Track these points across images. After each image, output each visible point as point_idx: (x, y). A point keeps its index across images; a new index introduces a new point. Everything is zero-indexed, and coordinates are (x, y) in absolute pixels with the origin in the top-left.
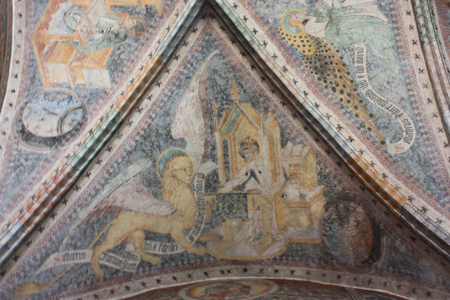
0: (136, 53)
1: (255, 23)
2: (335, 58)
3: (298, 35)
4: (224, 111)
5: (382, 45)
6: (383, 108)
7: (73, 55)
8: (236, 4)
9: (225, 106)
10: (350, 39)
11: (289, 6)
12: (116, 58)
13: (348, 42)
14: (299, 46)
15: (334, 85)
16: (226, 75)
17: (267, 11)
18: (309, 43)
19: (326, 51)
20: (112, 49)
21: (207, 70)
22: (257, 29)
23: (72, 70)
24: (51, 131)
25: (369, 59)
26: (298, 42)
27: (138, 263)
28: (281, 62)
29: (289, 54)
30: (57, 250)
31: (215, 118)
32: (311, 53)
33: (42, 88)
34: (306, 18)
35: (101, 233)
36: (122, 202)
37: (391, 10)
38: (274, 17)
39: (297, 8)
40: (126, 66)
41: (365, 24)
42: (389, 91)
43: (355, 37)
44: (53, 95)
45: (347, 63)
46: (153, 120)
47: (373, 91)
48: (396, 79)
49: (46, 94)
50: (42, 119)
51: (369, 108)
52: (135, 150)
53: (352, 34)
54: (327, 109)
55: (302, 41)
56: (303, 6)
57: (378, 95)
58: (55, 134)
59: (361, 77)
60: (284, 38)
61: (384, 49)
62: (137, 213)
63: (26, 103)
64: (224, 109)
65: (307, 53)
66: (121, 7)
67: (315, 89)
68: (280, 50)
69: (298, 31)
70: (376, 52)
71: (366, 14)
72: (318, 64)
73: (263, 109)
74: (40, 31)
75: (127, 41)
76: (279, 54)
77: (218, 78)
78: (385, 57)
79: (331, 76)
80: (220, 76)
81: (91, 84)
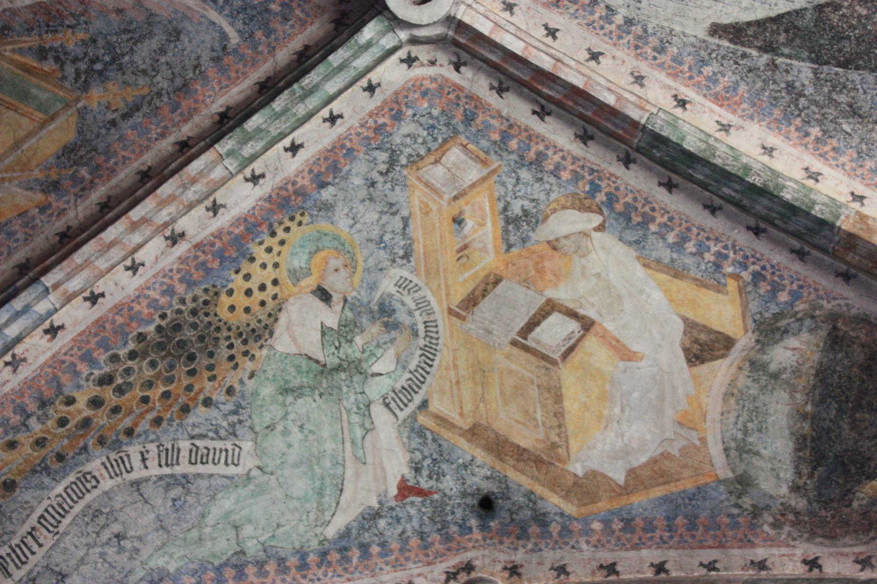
1: (320, 147)
2: (208, 385)
3: (282, 274)
4: (56, 67)
5: (250, 521)
6: (33, 520)
8: (378, 90)
9: (70, 70)
10: (271, 427)
11: (372, 246)
13: (260, 421)
14: (247, 277)
15: (120, 381)
16: (164, 67)
17: (357, 181)
18: (256, 308)
19: (231, 358)
21: (176, 12)
22: (302, 154)
25: (203, 483)
26: (260, 276)
28: (196, 225)
29: (222, 251)
31: (33, 40)
32: (224, 314)
34: (336, 297)
37: (364, 548)
38: (340, 204)
39: (367, 270)
41: (318, 471)
42: (89, 540)
43: (276, 442)
45: (191, 419)
47: (96, 493)
48: (131, 558)
51: (35, 480)
53: (286, 432)
54: (42, 360)
55: (262, 288)
56: (373, 287)
57: (78, 508)
59: (144, 460)
60: (273, 234)
61: (236, 528)
64: (62, 65)
65: (225, 300)
67: (108, 326)
68: (237, 222)
69: (296, 276)
70: (227, 503)
71: (349, 473)
72: (189, 334)
73: (54, 176)
76: (224, 219)
77: (154, 43)
78: (207, 530)
79: (148, 373)
80: (162, 51)
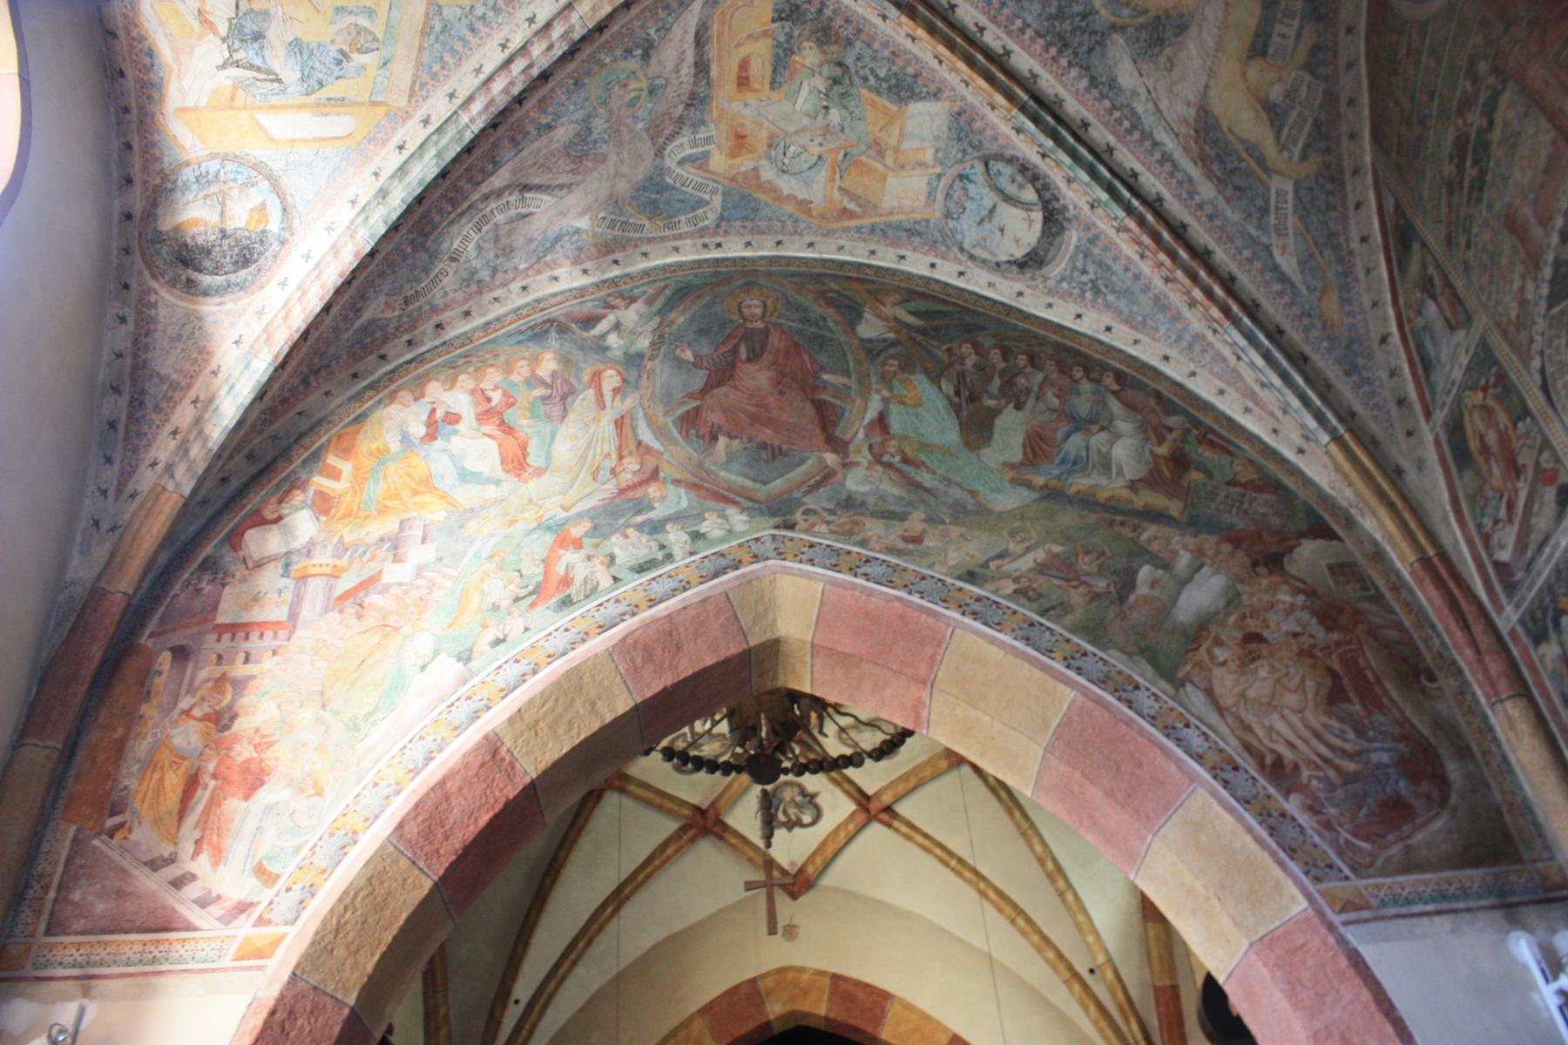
0: (876, 46)
7: (871, 162)
12: (884, 85)
20: (864, 92)
23: (903, 167)
24: (1031, 222)
27: (1308, 78)
30: (1268, 248)
33: (932, 221)
35: (1244, 155)
36: (1189, 105)
40: (904, 68)
44: (951, 205)
46: (1029, 26)
49: (948, 215)
50: (1002, 230)
52: (1088, 69)
58: (1038, 216)
62: (1212, 74)
63: (962, 249)
66: (775, 71)
74: (814, 213)
75: (849, 61)
81: (937, 138)
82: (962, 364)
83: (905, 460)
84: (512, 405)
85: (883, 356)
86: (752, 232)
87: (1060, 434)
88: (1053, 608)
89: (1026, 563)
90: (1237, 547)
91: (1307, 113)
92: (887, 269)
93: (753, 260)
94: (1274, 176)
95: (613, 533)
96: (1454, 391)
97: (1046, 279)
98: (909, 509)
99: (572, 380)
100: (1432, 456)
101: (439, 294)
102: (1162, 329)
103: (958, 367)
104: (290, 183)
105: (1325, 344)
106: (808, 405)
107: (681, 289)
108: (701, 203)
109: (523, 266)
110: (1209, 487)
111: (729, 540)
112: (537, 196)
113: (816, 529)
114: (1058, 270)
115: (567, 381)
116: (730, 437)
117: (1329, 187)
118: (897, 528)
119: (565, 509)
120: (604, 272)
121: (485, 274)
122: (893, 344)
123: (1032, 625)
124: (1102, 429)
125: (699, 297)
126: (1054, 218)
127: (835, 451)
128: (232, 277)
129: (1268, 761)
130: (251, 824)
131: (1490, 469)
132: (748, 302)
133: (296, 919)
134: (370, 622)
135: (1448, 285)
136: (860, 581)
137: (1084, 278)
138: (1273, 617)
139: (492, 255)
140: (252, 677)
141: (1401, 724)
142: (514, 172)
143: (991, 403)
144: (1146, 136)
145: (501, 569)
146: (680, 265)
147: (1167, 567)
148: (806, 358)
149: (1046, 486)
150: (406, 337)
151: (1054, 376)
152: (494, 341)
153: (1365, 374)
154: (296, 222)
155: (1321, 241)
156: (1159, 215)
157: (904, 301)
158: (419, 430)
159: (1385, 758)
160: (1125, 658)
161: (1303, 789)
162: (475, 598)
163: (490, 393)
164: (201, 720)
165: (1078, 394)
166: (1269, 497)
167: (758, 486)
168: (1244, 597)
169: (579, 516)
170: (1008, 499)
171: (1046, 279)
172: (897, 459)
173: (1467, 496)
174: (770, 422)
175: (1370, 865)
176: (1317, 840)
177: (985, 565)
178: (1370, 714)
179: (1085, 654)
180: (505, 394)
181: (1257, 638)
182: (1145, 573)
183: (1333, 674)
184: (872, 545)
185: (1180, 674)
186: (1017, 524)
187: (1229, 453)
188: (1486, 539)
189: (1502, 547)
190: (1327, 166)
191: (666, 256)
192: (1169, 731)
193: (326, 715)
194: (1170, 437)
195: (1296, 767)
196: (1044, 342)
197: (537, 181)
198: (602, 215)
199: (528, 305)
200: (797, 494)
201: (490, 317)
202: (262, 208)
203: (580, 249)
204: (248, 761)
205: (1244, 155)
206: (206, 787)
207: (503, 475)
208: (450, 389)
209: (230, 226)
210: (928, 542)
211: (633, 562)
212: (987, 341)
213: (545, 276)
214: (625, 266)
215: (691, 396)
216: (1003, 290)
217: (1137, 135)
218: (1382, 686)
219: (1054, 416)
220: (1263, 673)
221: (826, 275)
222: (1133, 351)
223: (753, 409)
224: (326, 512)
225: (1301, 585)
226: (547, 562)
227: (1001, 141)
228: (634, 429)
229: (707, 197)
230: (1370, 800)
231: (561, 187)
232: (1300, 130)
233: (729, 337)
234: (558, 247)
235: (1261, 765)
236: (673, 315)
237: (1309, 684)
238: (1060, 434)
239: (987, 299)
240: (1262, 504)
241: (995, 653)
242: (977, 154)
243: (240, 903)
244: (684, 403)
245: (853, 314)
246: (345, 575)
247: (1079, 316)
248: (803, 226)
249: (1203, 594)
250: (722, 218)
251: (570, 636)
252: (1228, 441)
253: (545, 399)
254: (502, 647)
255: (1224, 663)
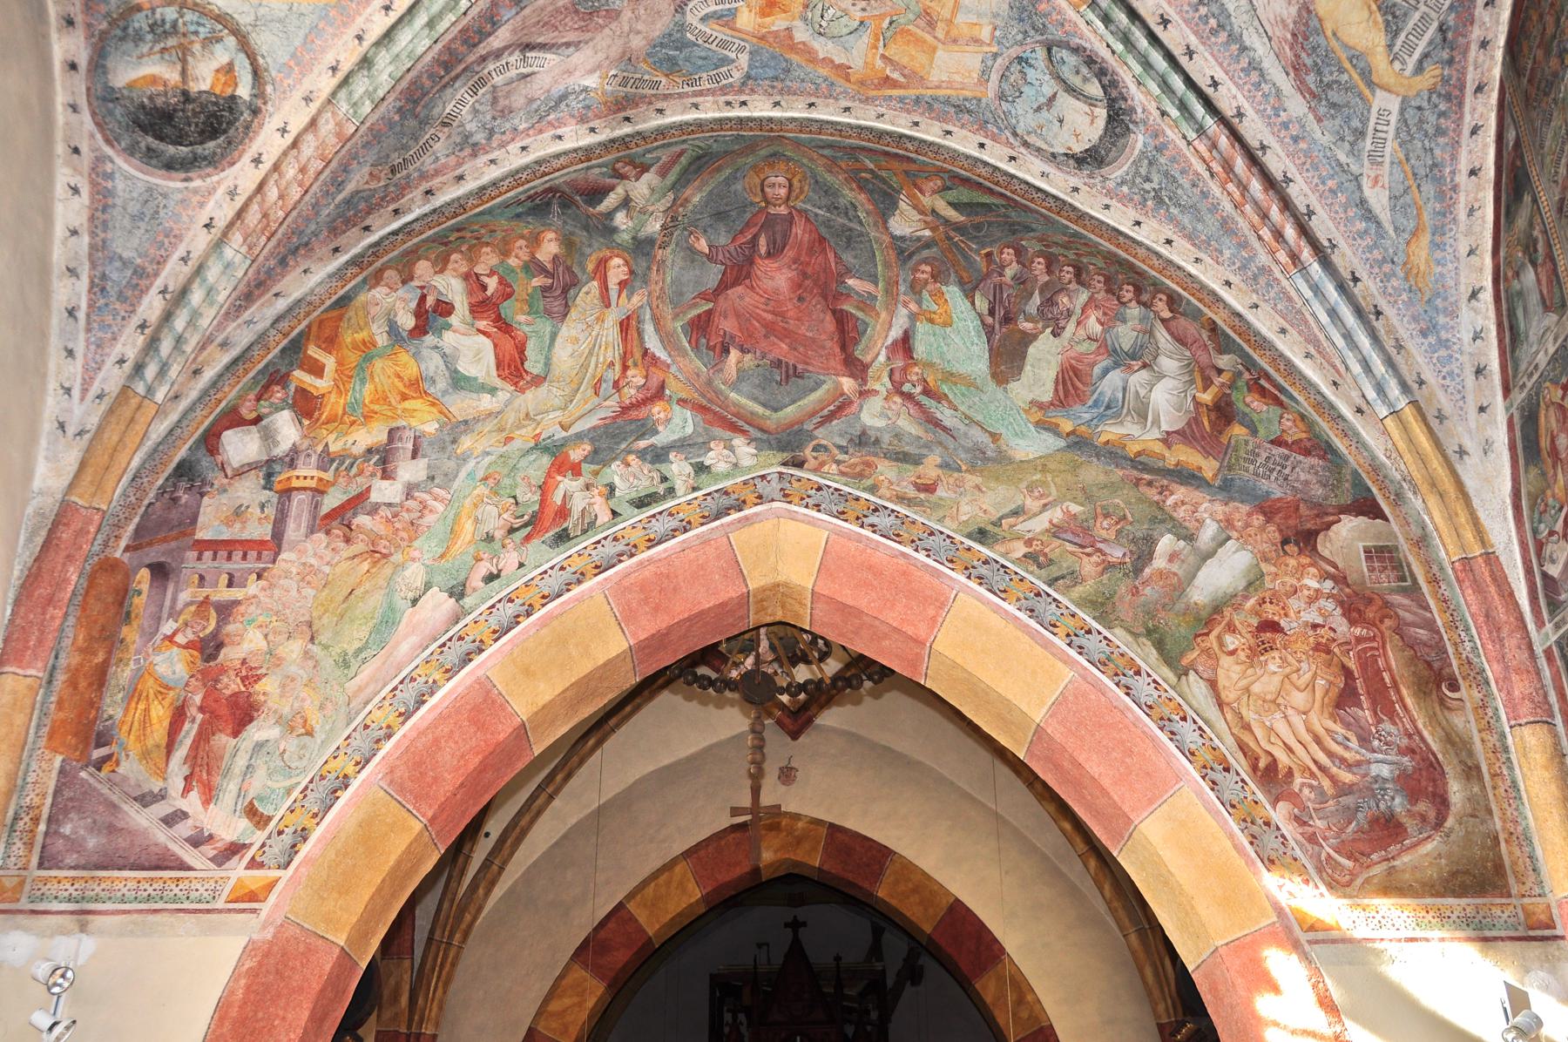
23: (955, 41)
30: (1357, 178)
35: (1347, 65)
44: (1005, 86)
49: (1002, 97)
50: (1061, 121)
58: (1102, 113)
63: (1015, 134)
82: (1001, 275)
83: (927, 392)
84: (509, 296)
85: (916, 258)
86: (781, 92)
87: (1097, 370)
88: (1063, 577)
89: (1039, 524)
90: (1269, 520)
91: (1433, 15)
92: (932, 144)
93: (780, 121)
94: (1378, 92)
95: (615, 459)
96: (1535, 377)
97: (1105, 179)
98: (925, 451)
99: (576, 269)
100: (1501, 436)
101: (429, 161)
102: (1227, 253)
103: (996, 279)
104: (263, 41)
105: (1405, 296)
106: (829, 317)
107: (699, 158)
108: (725, 61)
109: (521, 128)
110: (1250, 447)
111: (734, 476)
112: (541, 55)
113: (826, 468)
114: (1119, 173)
115: (569, 269)
116: (743, 351)
117: (1443, 107)
118: (911, 472)
119: (564, 428)
120: (613, 129)
121: (480, 137)
122: (928, 245)
123: (1038, 595)
124: (1145, 366)
125: (719, 170)
126: (1119, 118)
127: (852, 375)
128: (199, 149)
129: (1262, 764)
130: (241, 762)
131: (1555, 475)
132: (773, 179)
133: (289, 863)
134: (359, 547)
135: (1550, 257)
136: (867, 532)
137: (1147, 186)
138: (1294, 604)
139: (489, 117)
140: (237, 603)
141: (1410, 736)
142: (514, 31)
143: (1027, 326)
144: (1234, 38)
145: (496, 493)
146: (700, 125)
147: (1190, 538)
148: (831, 256)
149: (1073, 432)
150: (392, 207)
151: (1101, 296)
152: (490, 212)
153: (1444, 335)
154: (269, 89)
155: (1422, 172)
156: (1236, 136)
157: (946, 188)
158: (407, 321)
159: (1385, 771)
160: (1130, 638)
161: (1294, 798)
162: (469, 526)
163: (486, 280)
164: (186, 647)
165: (1124, 321)
166: (1314, 461)
167: (768, 413)
168: (1267, 578)
169: (579, 437)
170: (1030, 445)
171: (1105, 179)
172: (919, 389)
173: (1529, 493)
174: (786, 335)
175: (1348, 884)
176: (1298, 853)
177: (997, 523)
178: (1380, 721)
179: (1089, 632)
180: (502, 281)
181: (1273, 627)
182: (1166, 543)
183: (1347, 672)
184: (883, 491)
185: (1185, 662)
186: (1038, 477)
187: (1281, 404)
188: (1540, 546)
189: (1553, 562)
190: (1445, 81)
191: (683, 113)
192: (1163, 722)
193: (315, 649)
194: (1218, 380)
195: (1290, 773)
196: (1095, 251)
197: (540, 40)
198: (613, 72)
199: (526, 167)
200: (808, 426)
201: (485, 180)
202: (229, 69)
203: (588, 107)
204: (236, 694)
205: (1347, 65)
206: (193, 721)
207: (498, 383)
208: (441, 271)
209: (194, 88)
210: (941, 492)
211: (634, 495)
212: (1032, 246)
213: (548, 135)
214: (637, 123)
215: (704, 296)
216: (1059, 183)
217: (1223, 36)
218: (1398, 692)
219: (1095, 345)
220: (1272, 667)
221: (864, 149)
222: (1192, 269)
223: (769, 317)
224: (309, 415)
225: (1332, 570)
226: (545, 489)
227: (1067, 27)
228: (640, 333)
229: (733, 56)
230: (1360, 815)
231: (568, 45)
232: (1420, 36)
233: (748, 225)
234: (563, 106)
235: (1255, 768)
236: (688, 192)
237: (1320, 682)
238: (1097, 370)
239: (1039, 190)
240: (1306, 471)
241: (995, 621)
242: (1039, 38)
243: (232, 844)
244: (695, 305)
245: (886, 203)
246: (331, 490)
247: (1138, 223)
248: (839, 90)
249: (1224, 572)
250: (748, 77)
251: (566, 576)
252: (1282, 390)
253: (545, 290)
254: (496, 583)
255: (1232, 653)
